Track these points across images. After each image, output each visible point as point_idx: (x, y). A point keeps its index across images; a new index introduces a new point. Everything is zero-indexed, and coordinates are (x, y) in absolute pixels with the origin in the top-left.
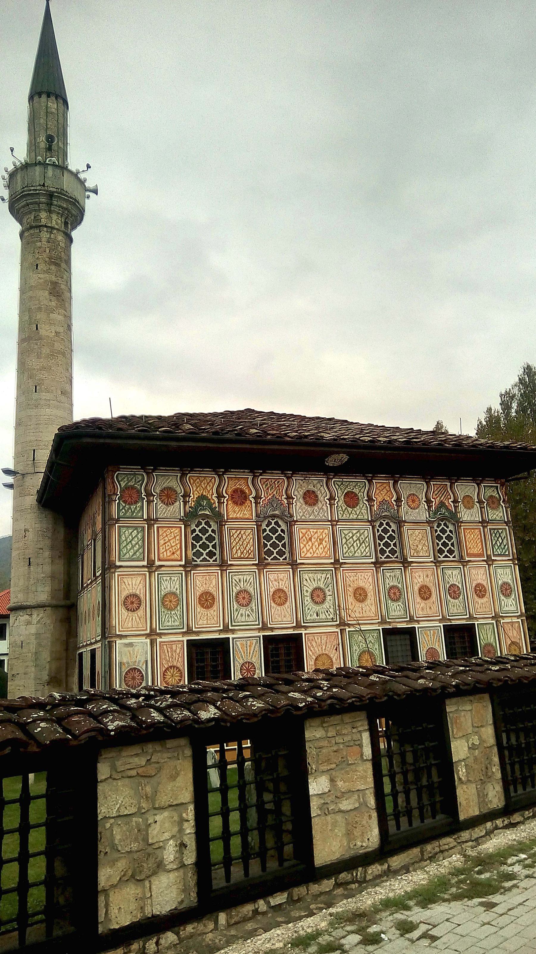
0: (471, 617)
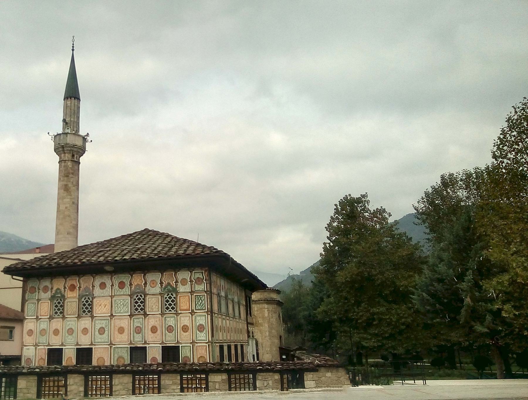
0: (178, 342)
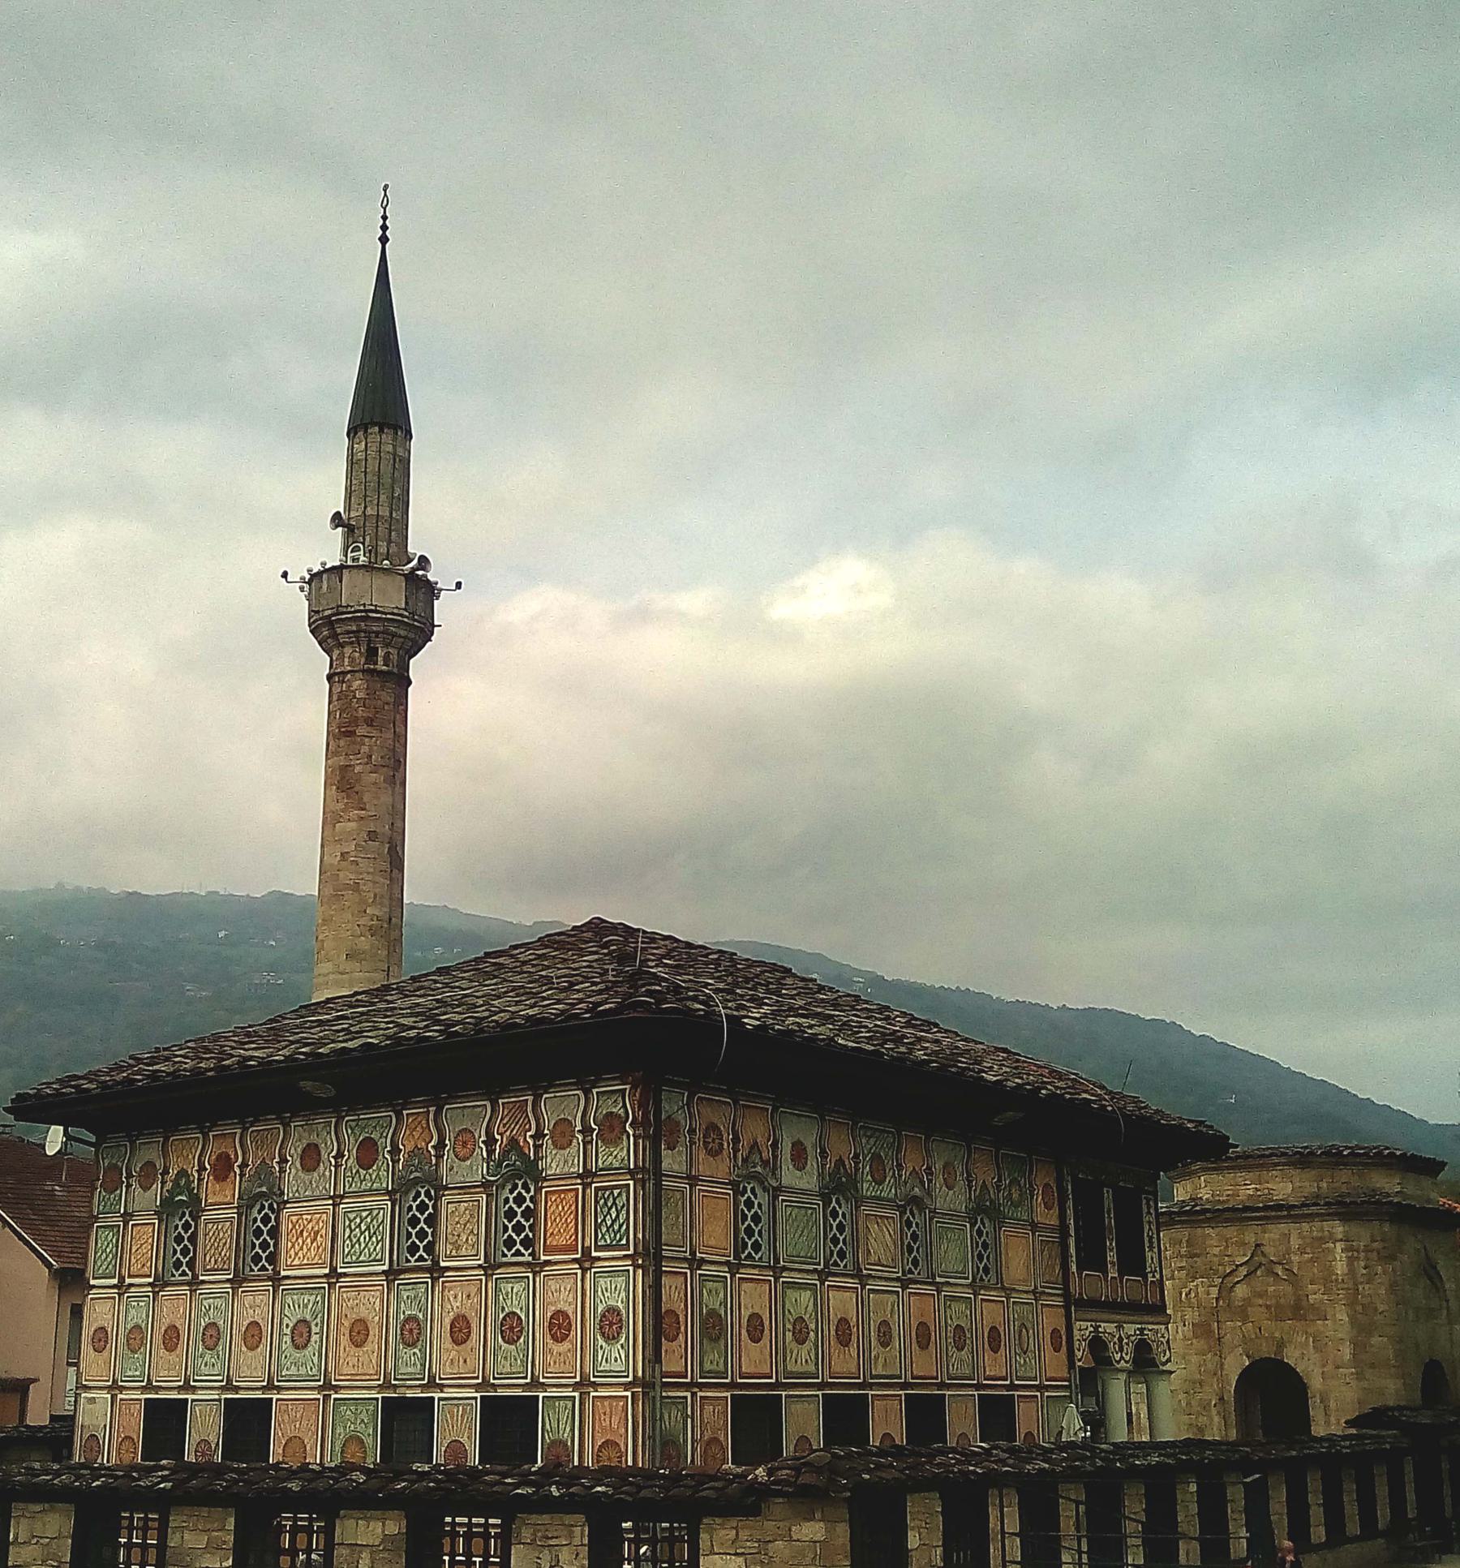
0: (535, 1384)
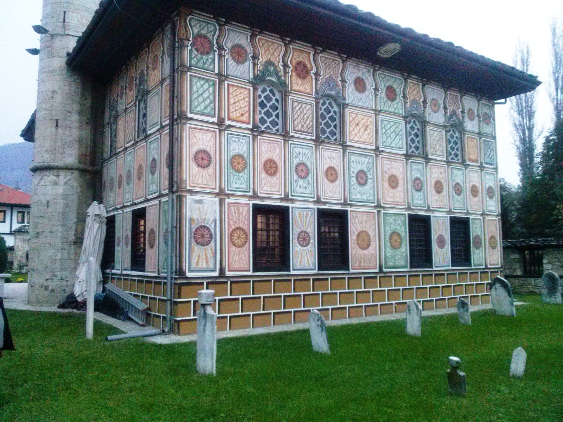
0: (468, 213)
